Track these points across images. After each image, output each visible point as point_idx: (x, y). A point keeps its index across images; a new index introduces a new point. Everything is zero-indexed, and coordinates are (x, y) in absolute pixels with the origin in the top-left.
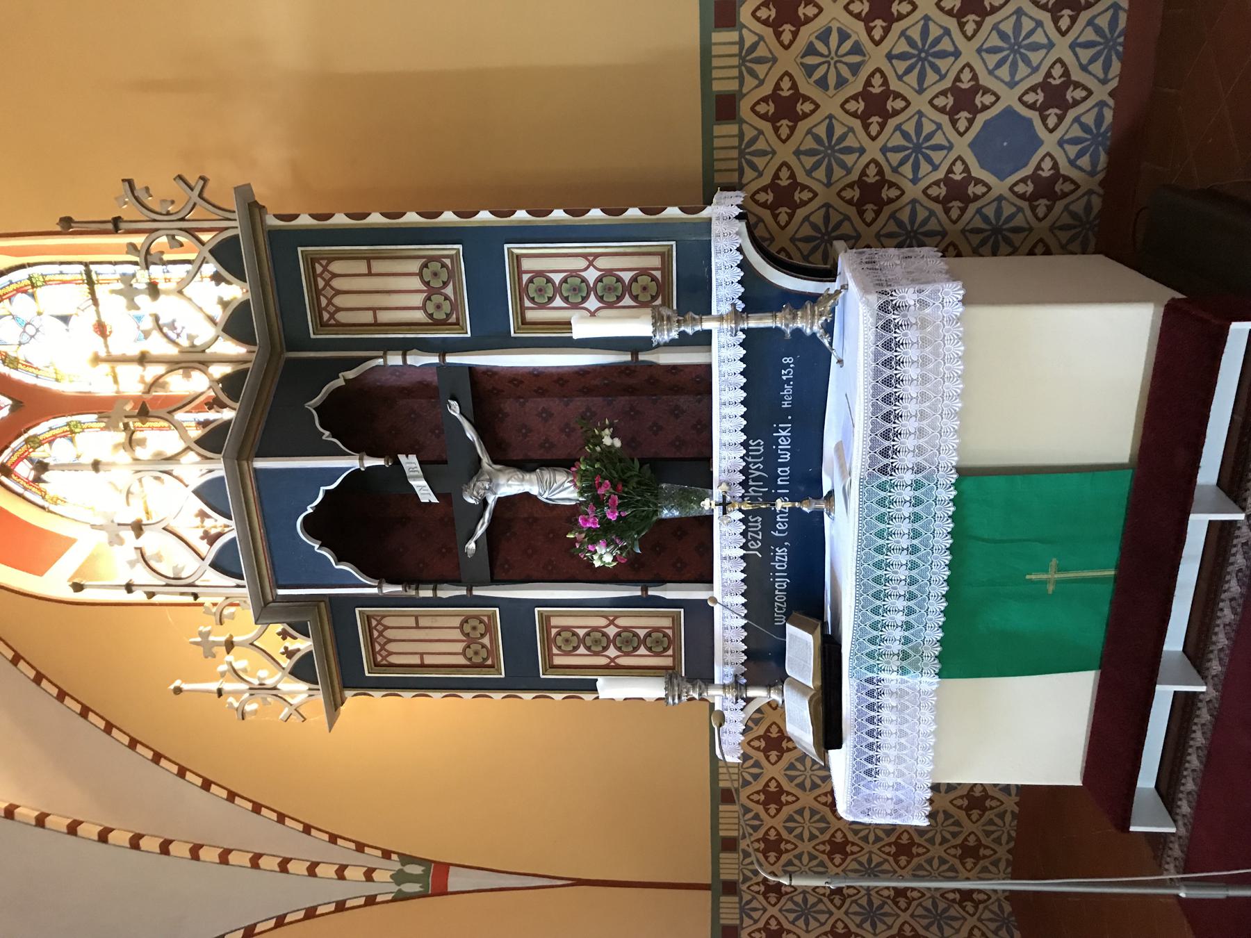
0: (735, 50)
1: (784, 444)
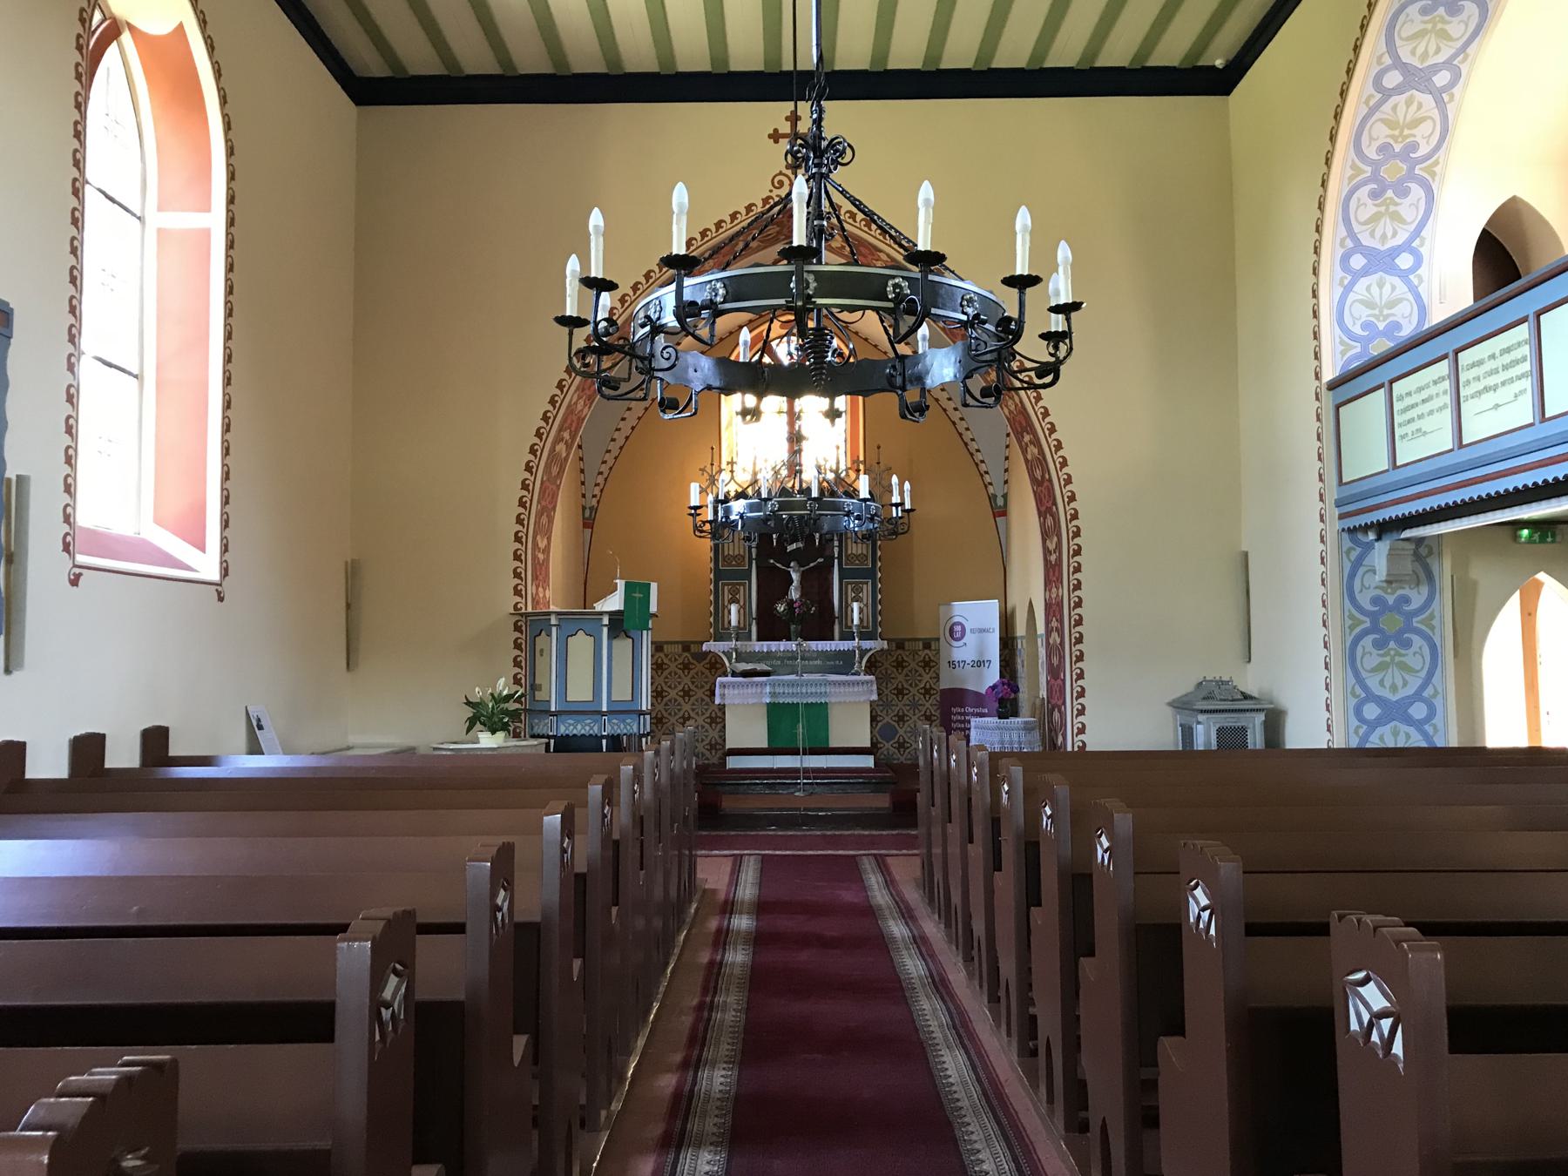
0: (917, 648)
1: (816, 662)
